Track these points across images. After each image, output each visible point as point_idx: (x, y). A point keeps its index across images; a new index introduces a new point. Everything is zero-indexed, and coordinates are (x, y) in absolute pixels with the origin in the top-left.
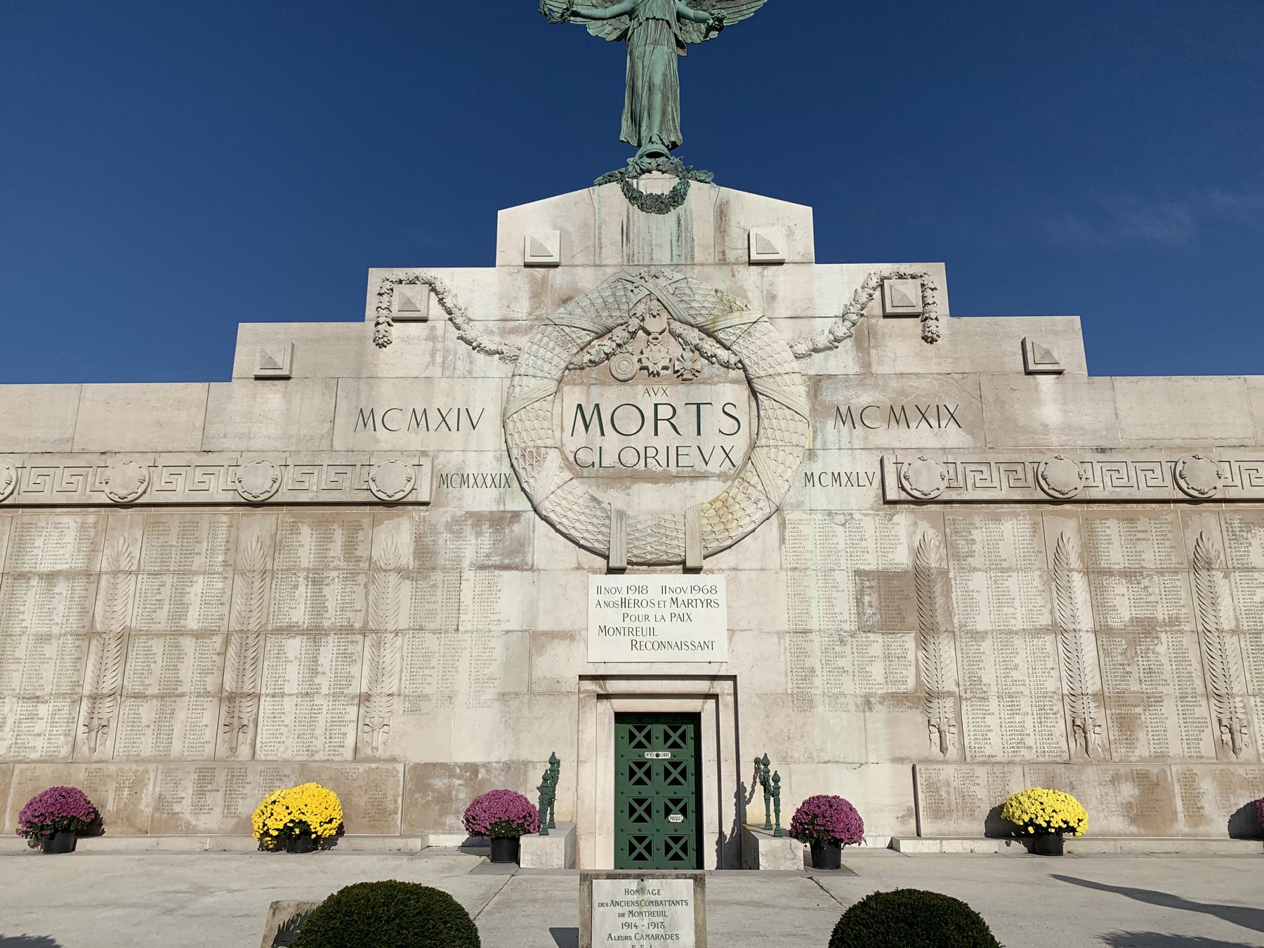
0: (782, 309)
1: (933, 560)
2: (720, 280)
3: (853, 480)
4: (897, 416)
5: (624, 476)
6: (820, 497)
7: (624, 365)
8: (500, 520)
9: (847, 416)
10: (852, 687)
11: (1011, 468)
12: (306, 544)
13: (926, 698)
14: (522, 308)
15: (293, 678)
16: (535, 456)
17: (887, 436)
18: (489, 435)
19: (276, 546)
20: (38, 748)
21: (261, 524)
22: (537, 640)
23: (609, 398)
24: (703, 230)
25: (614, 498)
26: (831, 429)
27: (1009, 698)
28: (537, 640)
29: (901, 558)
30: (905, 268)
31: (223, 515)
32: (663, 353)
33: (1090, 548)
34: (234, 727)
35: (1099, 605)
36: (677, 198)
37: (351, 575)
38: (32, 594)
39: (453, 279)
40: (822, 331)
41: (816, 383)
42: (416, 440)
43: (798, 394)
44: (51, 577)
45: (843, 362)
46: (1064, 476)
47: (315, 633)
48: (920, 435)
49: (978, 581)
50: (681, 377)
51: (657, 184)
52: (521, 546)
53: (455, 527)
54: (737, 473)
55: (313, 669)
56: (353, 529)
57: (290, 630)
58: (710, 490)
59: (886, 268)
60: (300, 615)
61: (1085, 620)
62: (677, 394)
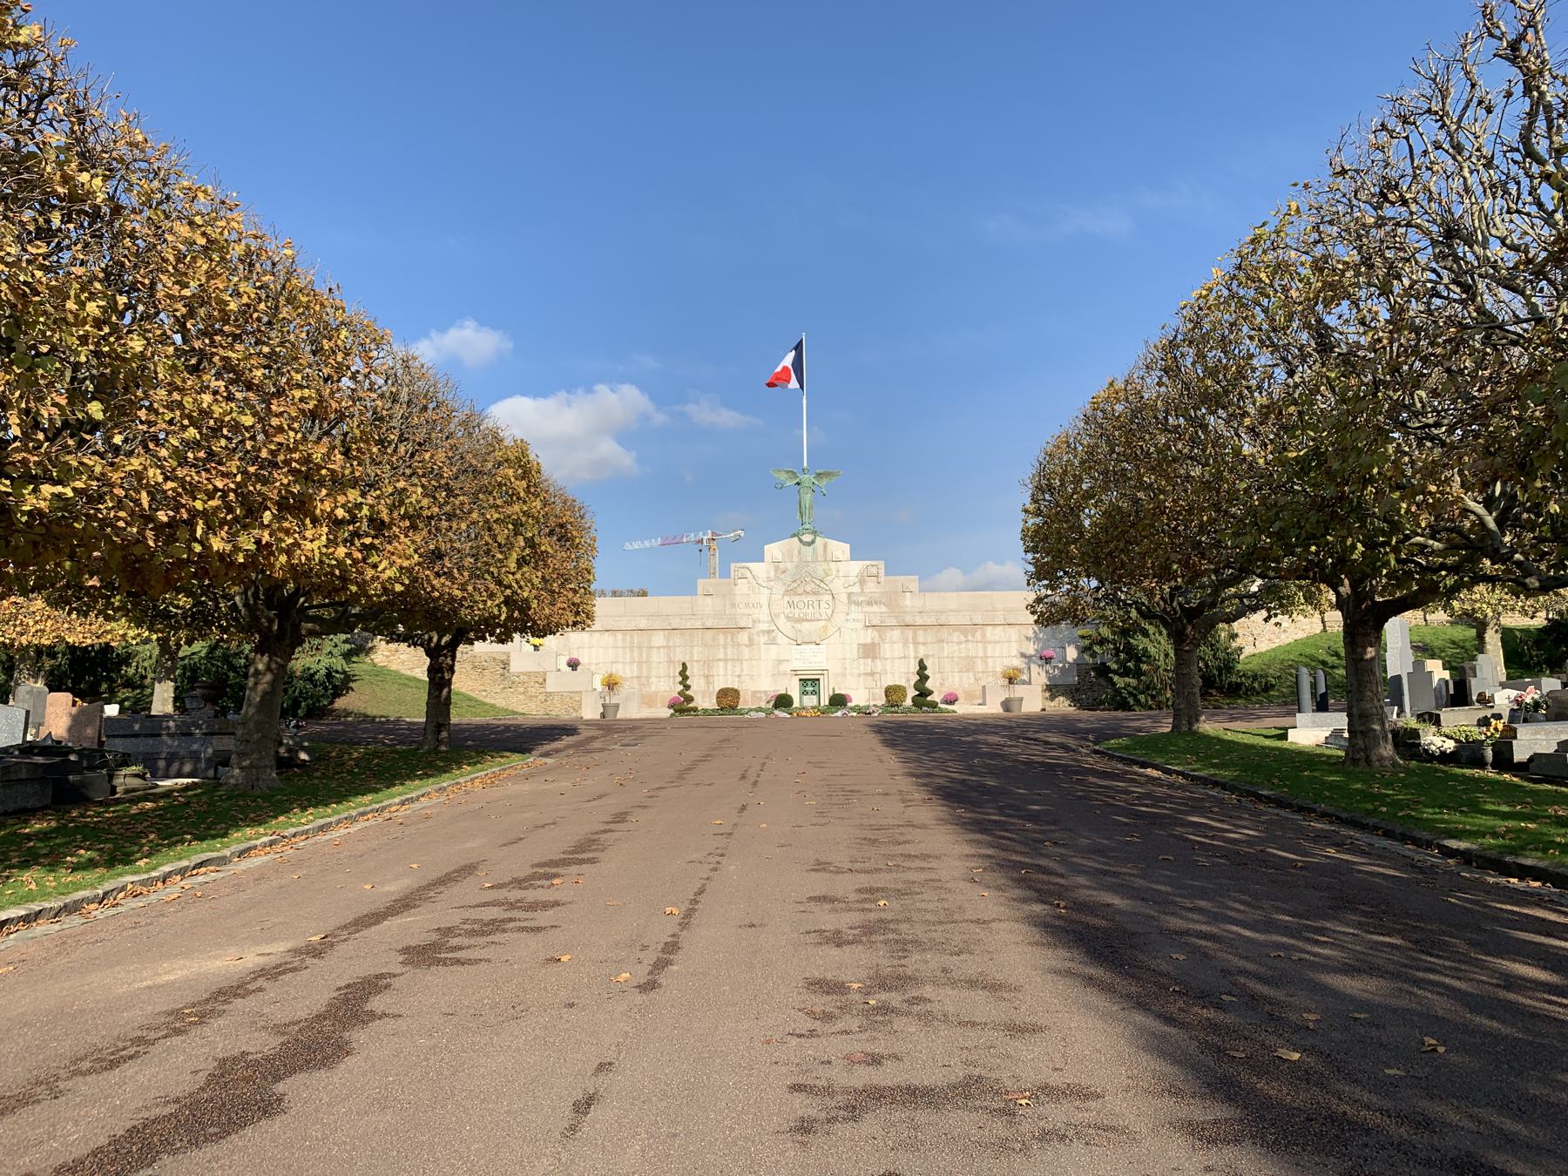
0: (841, 574)
1: (876, 641)
2: (825, 566)
3: (858, 621)
4: (870, 603)
5: (800, 620)
6: (850, 625)
7: (800, 590)
8: (769, 632)
9: (858, 604)
10: (856, 672)
11: (896, 617)
12: (721, 638)
13: (872, 674)
14: (772, 574)
15: (721, 671)
16: (778, 615)
17: (870, 609)
18: (765, 609)
19: (714, 639)
20: (662, 689)
21: (709, 634)
22: (780, 662)
23: (796, 599)
24: (820, 551)
25: (798, 626)
26: (853, 607)
27: (893, 673)
28: (780, 662)
29: (869, 641)
30: (874, 563)
31: (700, 632)
32: (808, 588)
33: (915, 637)
34: (708, 683)
35: (916, 651)
36: (813, 542)
37: (733, 646)
38: (655, 652)
39: (753, 566)
40: (853, 579)
41: (850, 595)
42: (746, 611)
43: (844, 598)
44: (659, 648)
45: (856, 589)
46: (909, 620)
47: (726, 661)
48: (875, 608)
49: (887, 646)
50: (815, 593)
51: (807, 538)
52: (775, 638)
53: (758, 634)
54: (829, 619)
55: (726, 669)
56: (733, 635)
57: (720, 660)
58: (823, 623)
59: (868, 563)
60: (722, 656)
61: (912, 655)
62: (814, 598)
